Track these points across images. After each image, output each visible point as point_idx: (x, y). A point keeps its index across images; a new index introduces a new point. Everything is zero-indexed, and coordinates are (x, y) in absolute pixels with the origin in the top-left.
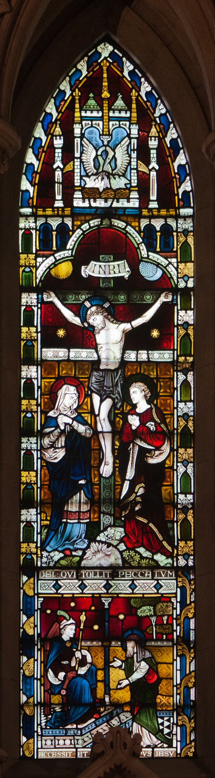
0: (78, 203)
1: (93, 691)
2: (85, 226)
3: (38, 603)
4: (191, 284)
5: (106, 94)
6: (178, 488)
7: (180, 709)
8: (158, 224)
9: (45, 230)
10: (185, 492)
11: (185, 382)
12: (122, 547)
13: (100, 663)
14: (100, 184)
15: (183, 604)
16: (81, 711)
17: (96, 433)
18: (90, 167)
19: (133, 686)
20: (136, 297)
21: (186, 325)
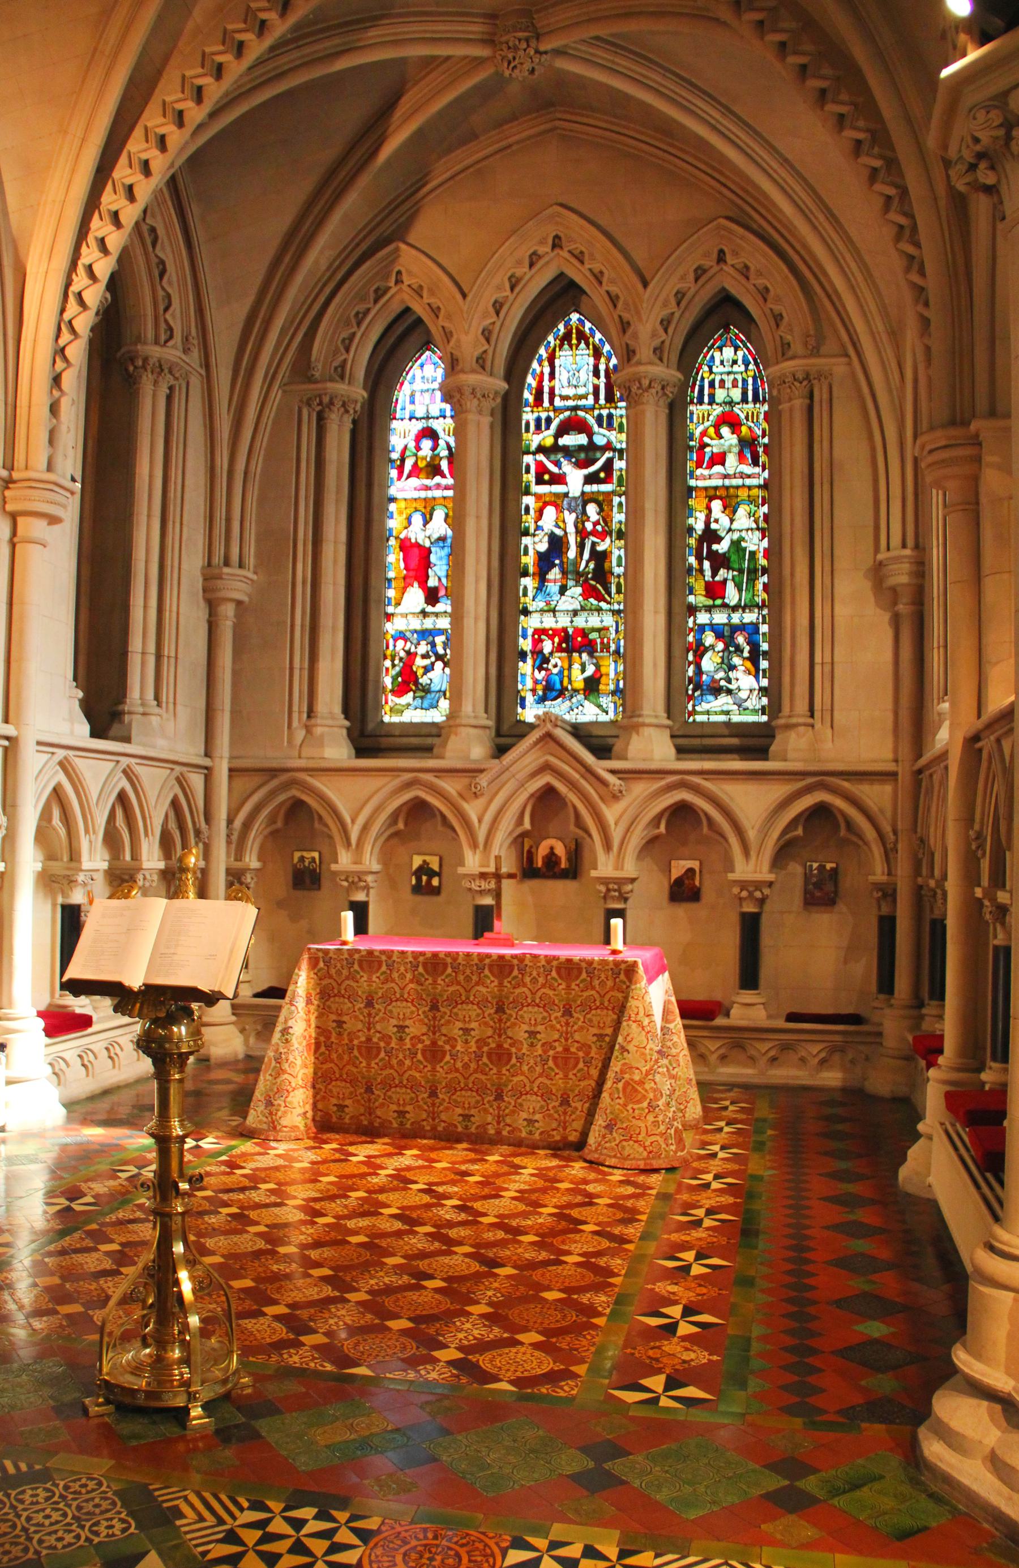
0: (558, 402)
1: (561, 682)
2: (562, 417)
3: (530, 632)
4: (624, 446)
5: (574, 341)
6: (614, 563)
7: (613, 693)
8: (605, 412)
9: (538, 420)
10: (619, 565)
11: (620, 504)
12: (581, 598)
13: (566, 666)
14: (570, 392)
15: (617, 631)
16: (554, 694)
17: (566, 533)
18: (565, 384)
19: (587, 680)
20: (591, 454)
21: (621, 470)
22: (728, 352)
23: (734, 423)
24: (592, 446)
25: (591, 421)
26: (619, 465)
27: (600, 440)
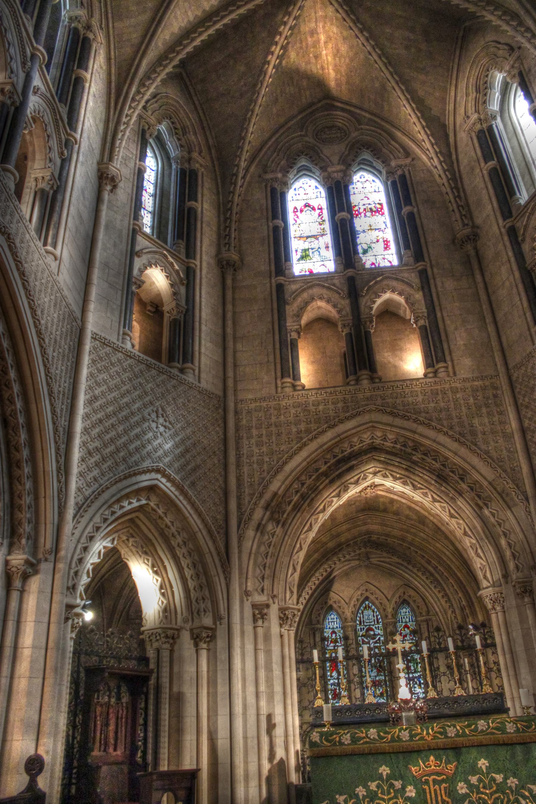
22: (404, 610)
23: (408, 628)
24: (375, 635)
25: (374, 628)
26: (382, 639)
27: (377, 633)
